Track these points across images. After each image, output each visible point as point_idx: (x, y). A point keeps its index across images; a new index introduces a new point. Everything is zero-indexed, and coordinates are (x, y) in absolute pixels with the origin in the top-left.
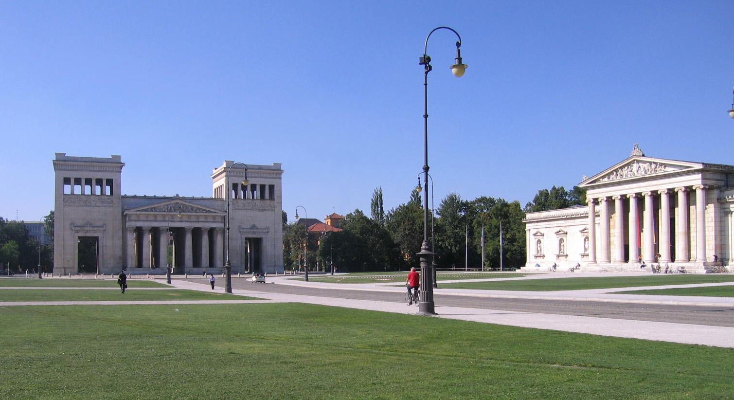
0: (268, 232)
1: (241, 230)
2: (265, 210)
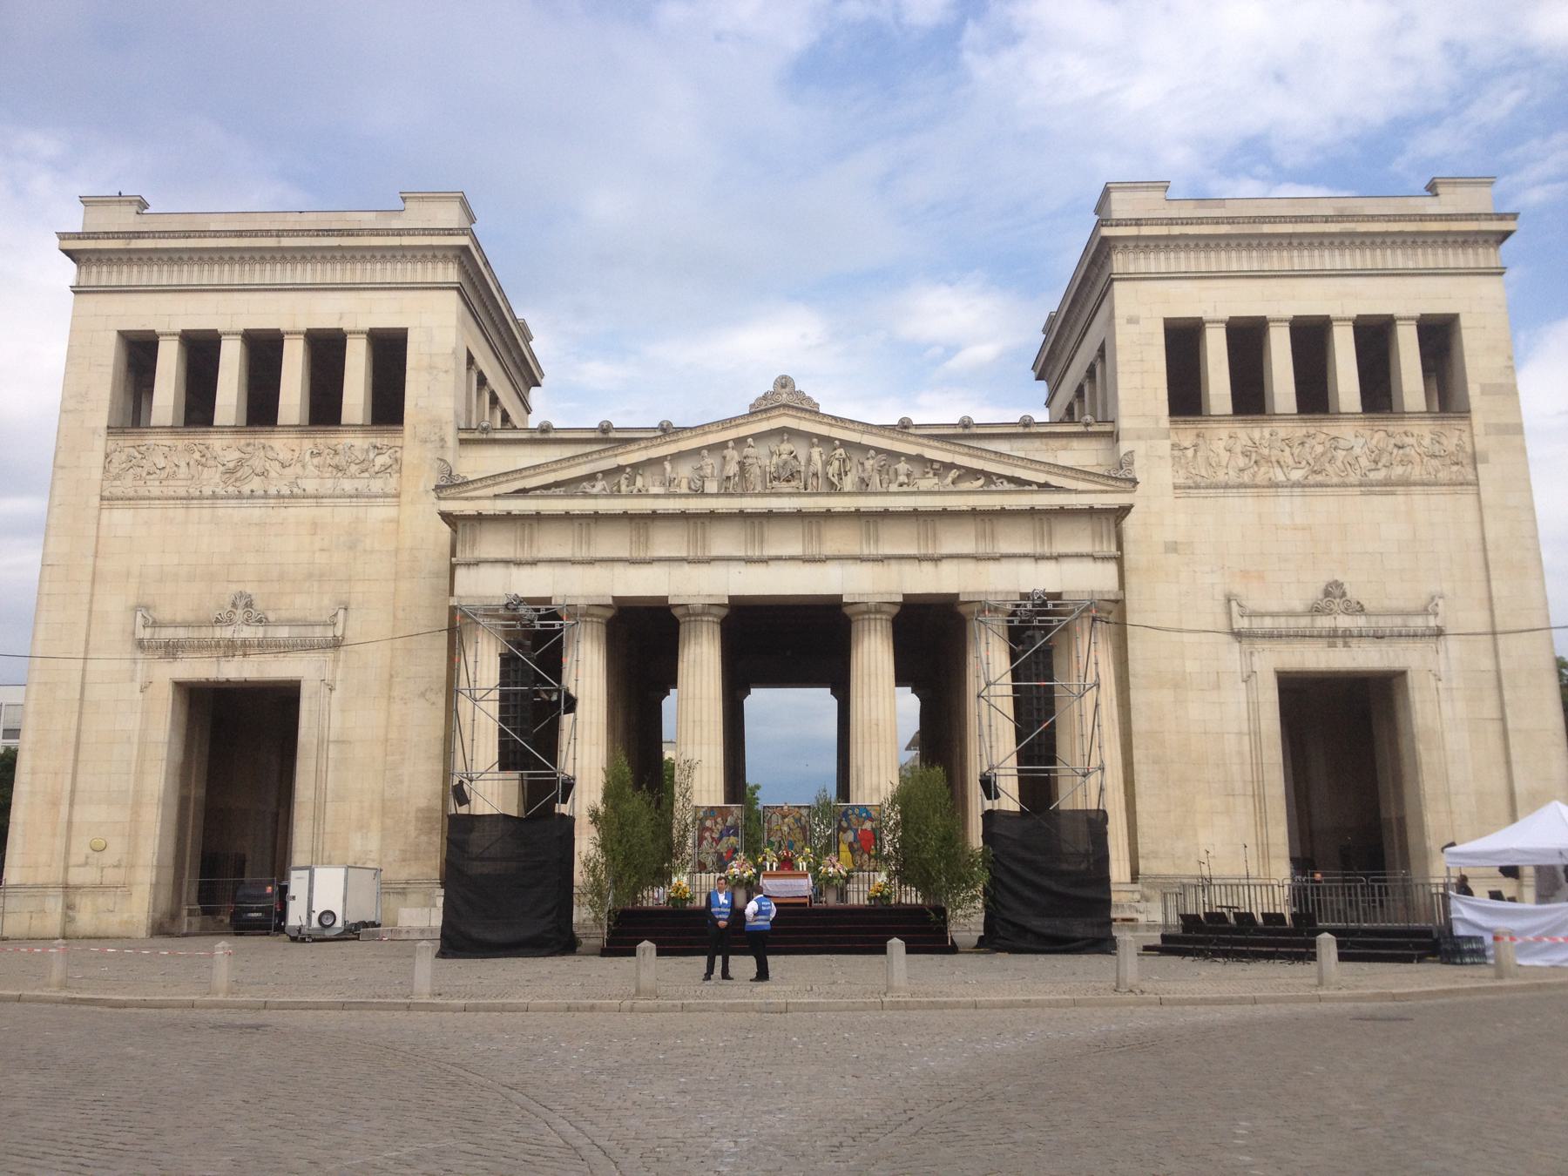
1: (1242, 624)
2: (1406, 483)
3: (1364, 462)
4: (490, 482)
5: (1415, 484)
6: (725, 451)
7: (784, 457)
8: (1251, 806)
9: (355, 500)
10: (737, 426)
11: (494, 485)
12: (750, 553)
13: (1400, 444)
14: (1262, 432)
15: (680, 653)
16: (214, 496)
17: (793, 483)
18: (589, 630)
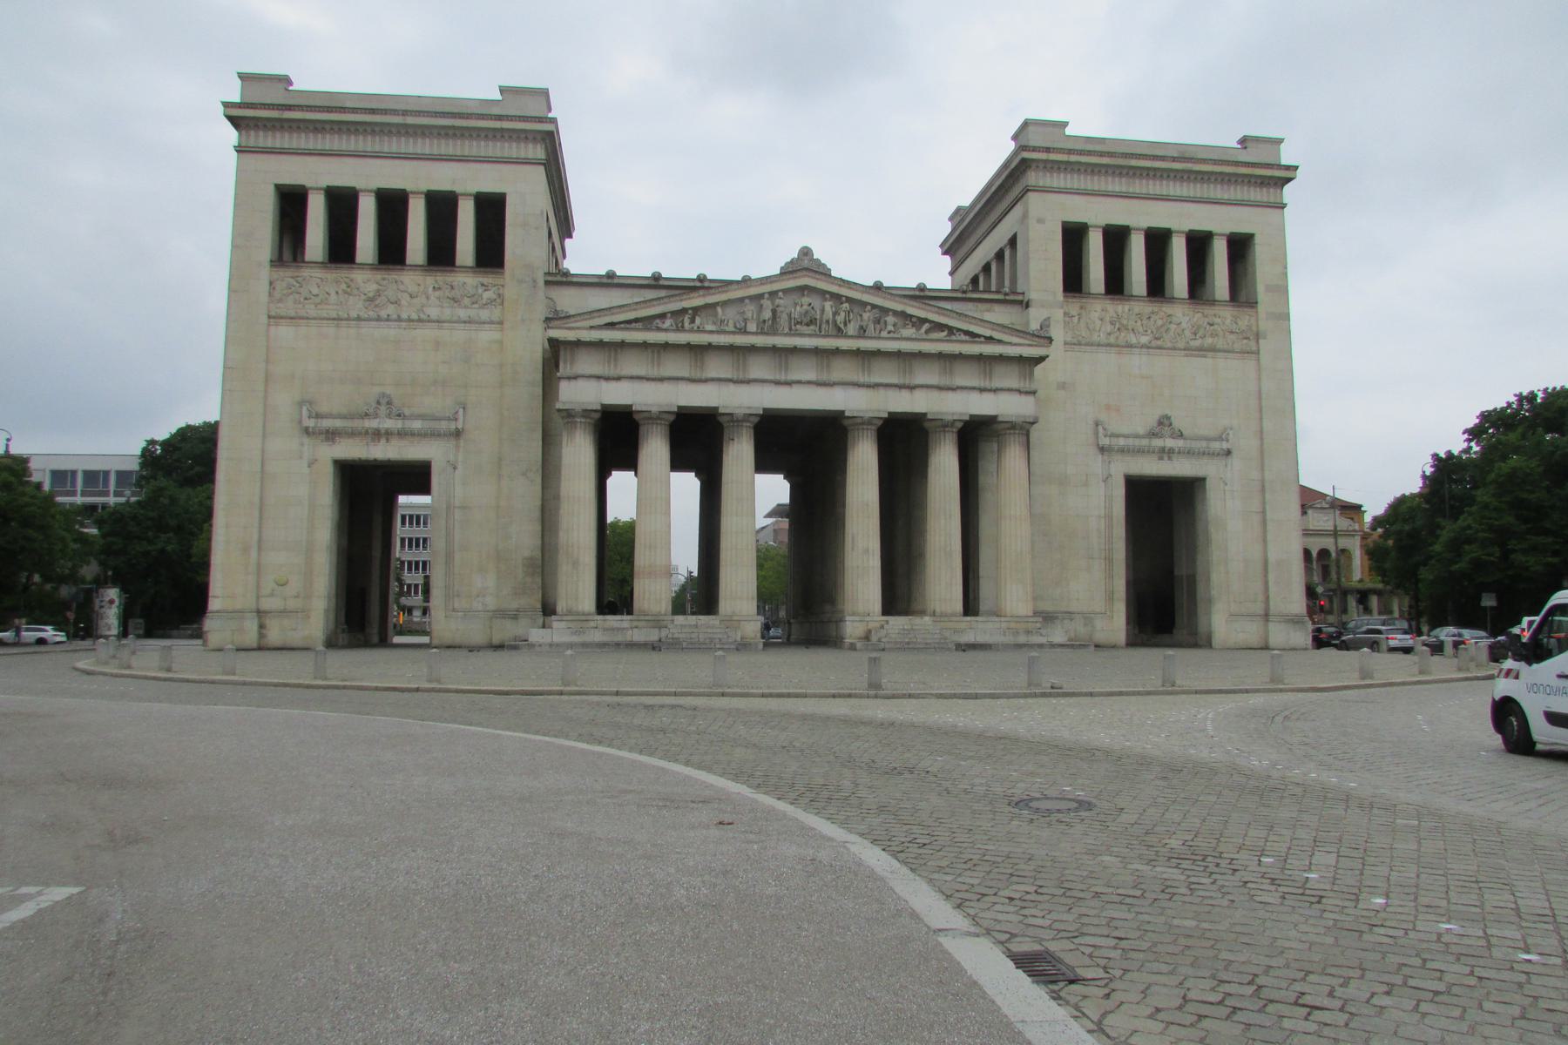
0: (1229, 453)
1: (1105, 441)
2: (1213, 349)
3: (1187, 333)
4: (586, 317)
5: (1219, 351)
6: (762, 302)
7: (805, 307)
8: (1103, 566)
9: (467, 325)
10: (771, 282)
11: (590, 319)
12: (778, 377)
13: (1211, 322)
14: (1123, 308)
15: (724, 449)
16: (359, 319)
17: (812, 327)
18: (659, 430)
